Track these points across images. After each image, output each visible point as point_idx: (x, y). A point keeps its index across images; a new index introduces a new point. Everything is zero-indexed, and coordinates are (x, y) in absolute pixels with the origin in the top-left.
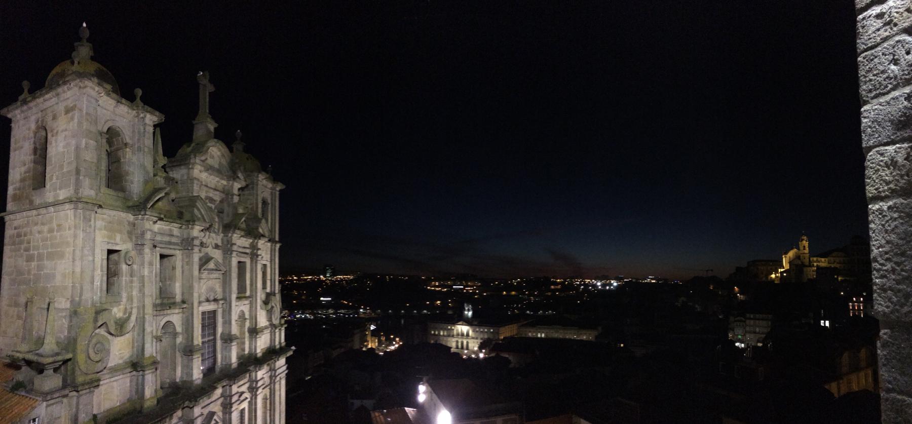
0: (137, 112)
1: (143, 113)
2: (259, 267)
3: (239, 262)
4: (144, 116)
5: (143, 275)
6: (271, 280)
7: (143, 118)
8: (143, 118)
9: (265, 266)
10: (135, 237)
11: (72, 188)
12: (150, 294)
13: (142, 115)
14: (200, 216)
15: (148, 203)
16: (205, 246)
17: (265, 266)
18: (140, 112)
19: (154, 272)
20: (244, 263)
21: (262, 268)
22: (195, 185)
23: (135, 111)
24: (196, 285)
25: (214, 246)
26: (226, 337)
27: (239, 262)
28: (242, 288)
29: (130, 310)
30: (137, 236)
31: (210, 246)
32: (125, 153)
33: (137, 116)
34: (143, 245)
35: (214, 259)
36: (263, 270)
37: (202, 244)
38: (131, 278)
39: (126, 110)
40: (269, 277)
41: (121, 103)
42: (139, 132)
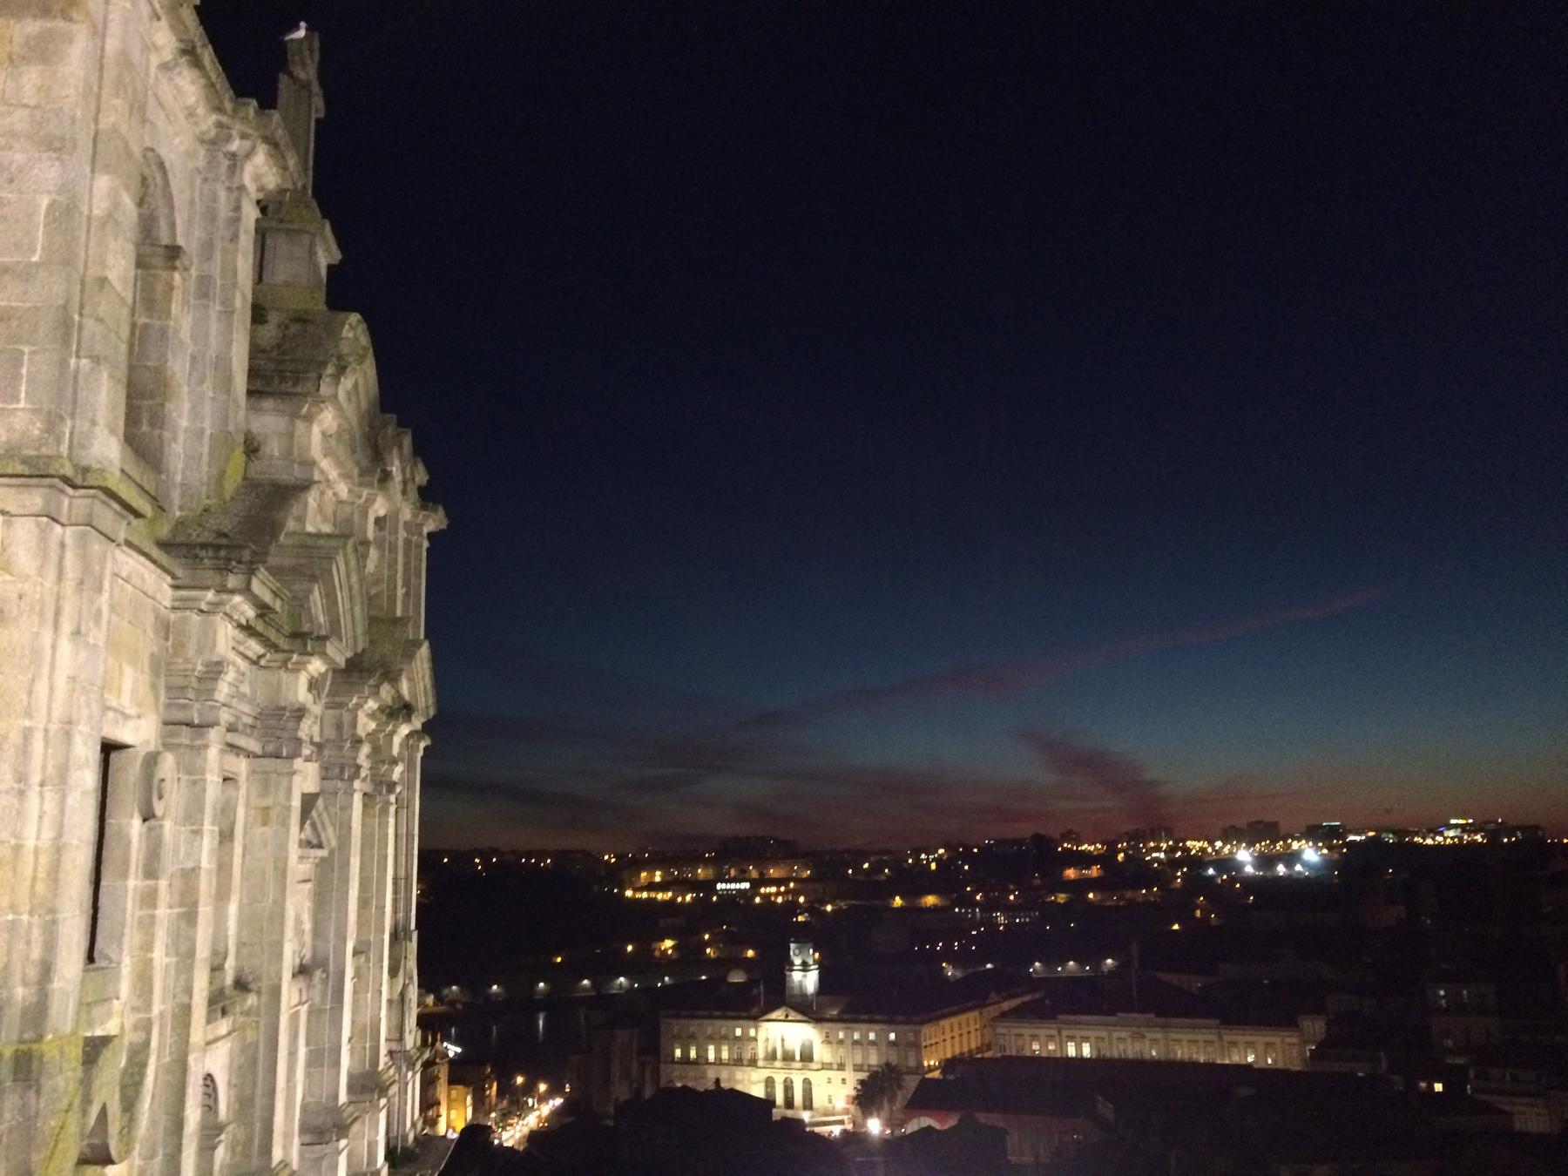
0: (220, 125)
1: (244, 136)
4: (241, 153)
5: (190, 865)
7: (235, 162)
8: (233, 156)
10: (169, 688)
11: (22, 405)
13: (235, 145)
14: (322, 619)
18: (238, 127)
23: (214, 117)
26: (318, 1121)
29: (138, 1037)
30: (180, 681)
32: (160, 288)
33: (213, 142)
34: (201, 727)
38: (151, 882)
39: (192, 100)
41: (196, 63)
42: (211, 215)
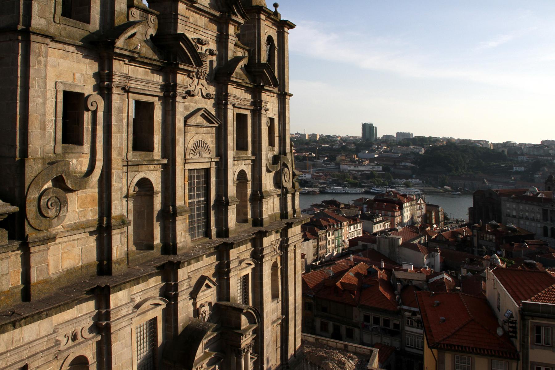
2: (264, 121)
3: (238, 115)
6: (279, 137)
9: (272, 120)
12: (118, 146)
15: (118, 38)
16: (192, 93)
17: (272, 120)
19: (125, 121)
20: (246, 116)
21: (267, 123)
22: (179, 21)
24: (180, 139)
25: (205, 95)
27: (238, 115)
28: (241, 146)
31: (200, 94)
35: (204, 109)
36: (269, 125)
37: (189, 93)
40: (276, 133)
